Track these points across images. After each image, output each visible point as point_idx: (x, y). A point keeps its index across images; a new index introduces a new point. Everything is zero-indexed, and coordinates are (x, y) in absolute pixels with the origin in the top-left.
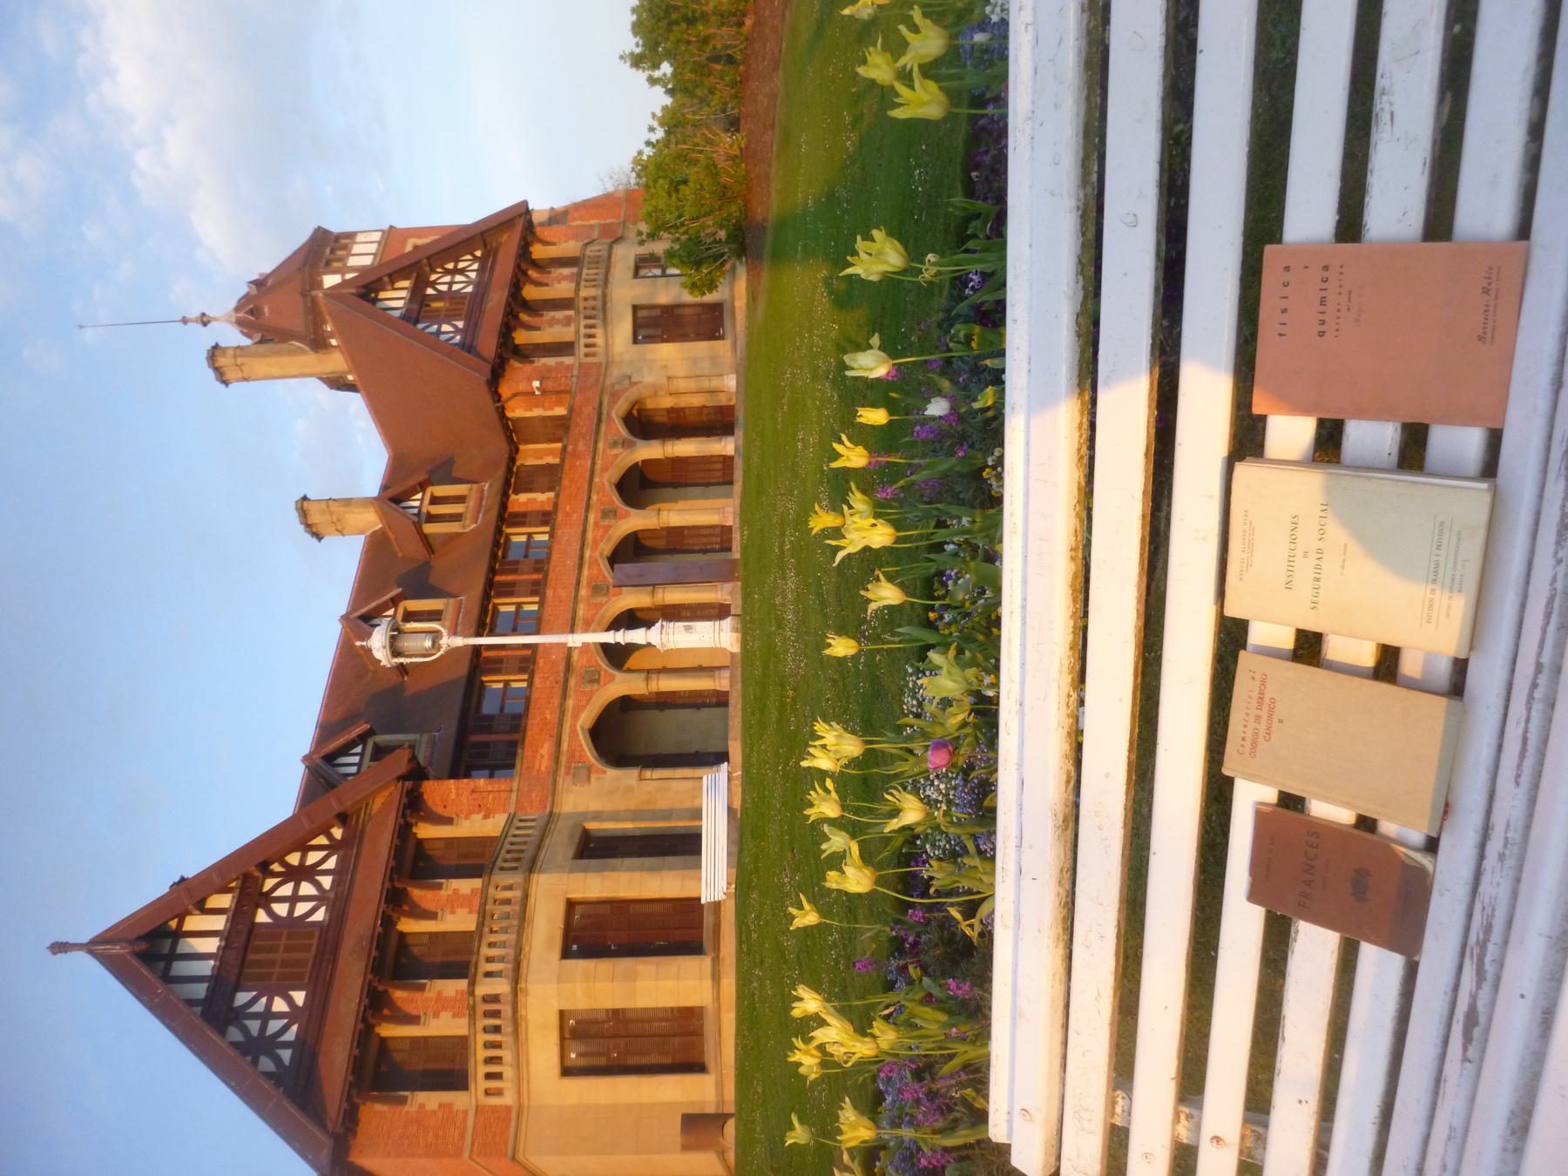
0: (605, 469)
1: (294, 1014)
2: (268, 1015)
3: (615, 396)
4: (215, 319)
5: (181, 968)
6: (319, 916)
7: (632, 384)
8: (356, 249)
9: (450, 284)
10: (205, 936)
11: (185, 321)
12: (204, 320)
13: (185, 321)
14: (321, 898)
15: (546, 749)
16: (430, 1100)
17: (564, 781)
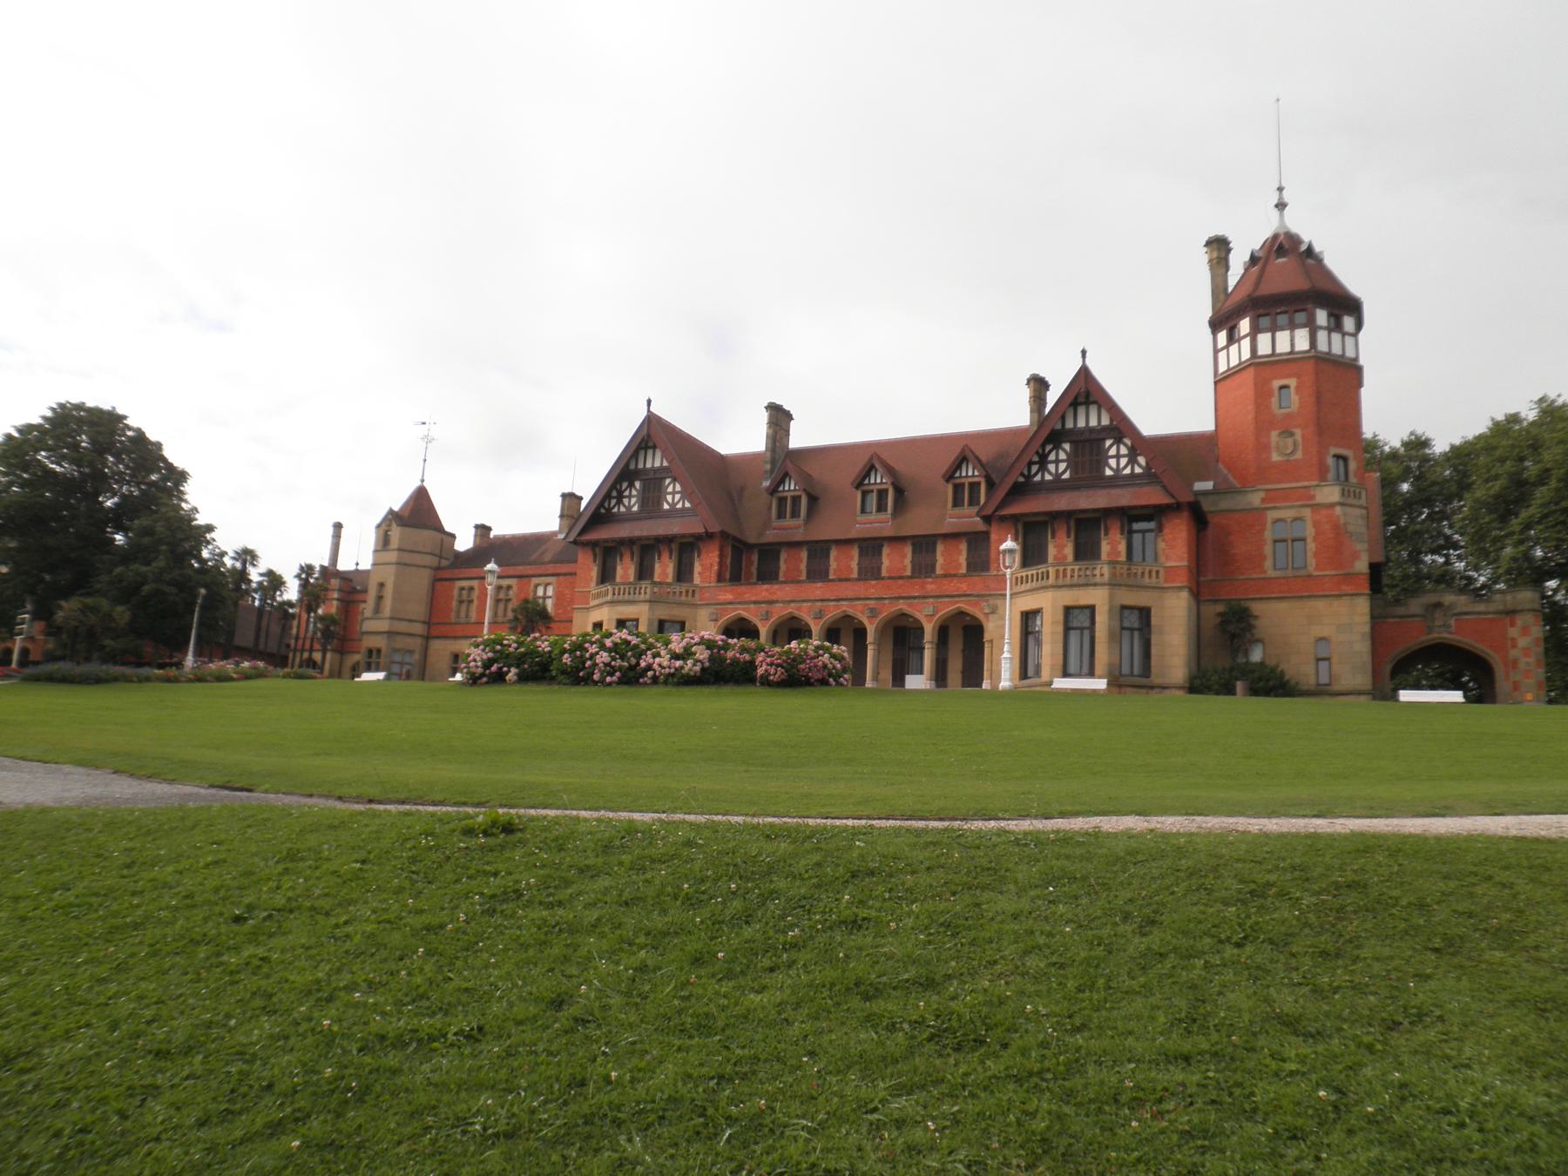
0: (910, 605)
1: (629, 508)
2: (630, 497)
3: (976, 604)
4: (1282, 216)
5: (650, 452)
6: (666, 506)
7: (987, 615)
8: (1283, 338)
9: (1118, 456)
10: (655, 461)
11: (1280, 189)
12: (1281, 206)
13: (1280, 189)
14: (673, 505)
15: (729, 597)
16: (594, 572)
17: (711, 610)
